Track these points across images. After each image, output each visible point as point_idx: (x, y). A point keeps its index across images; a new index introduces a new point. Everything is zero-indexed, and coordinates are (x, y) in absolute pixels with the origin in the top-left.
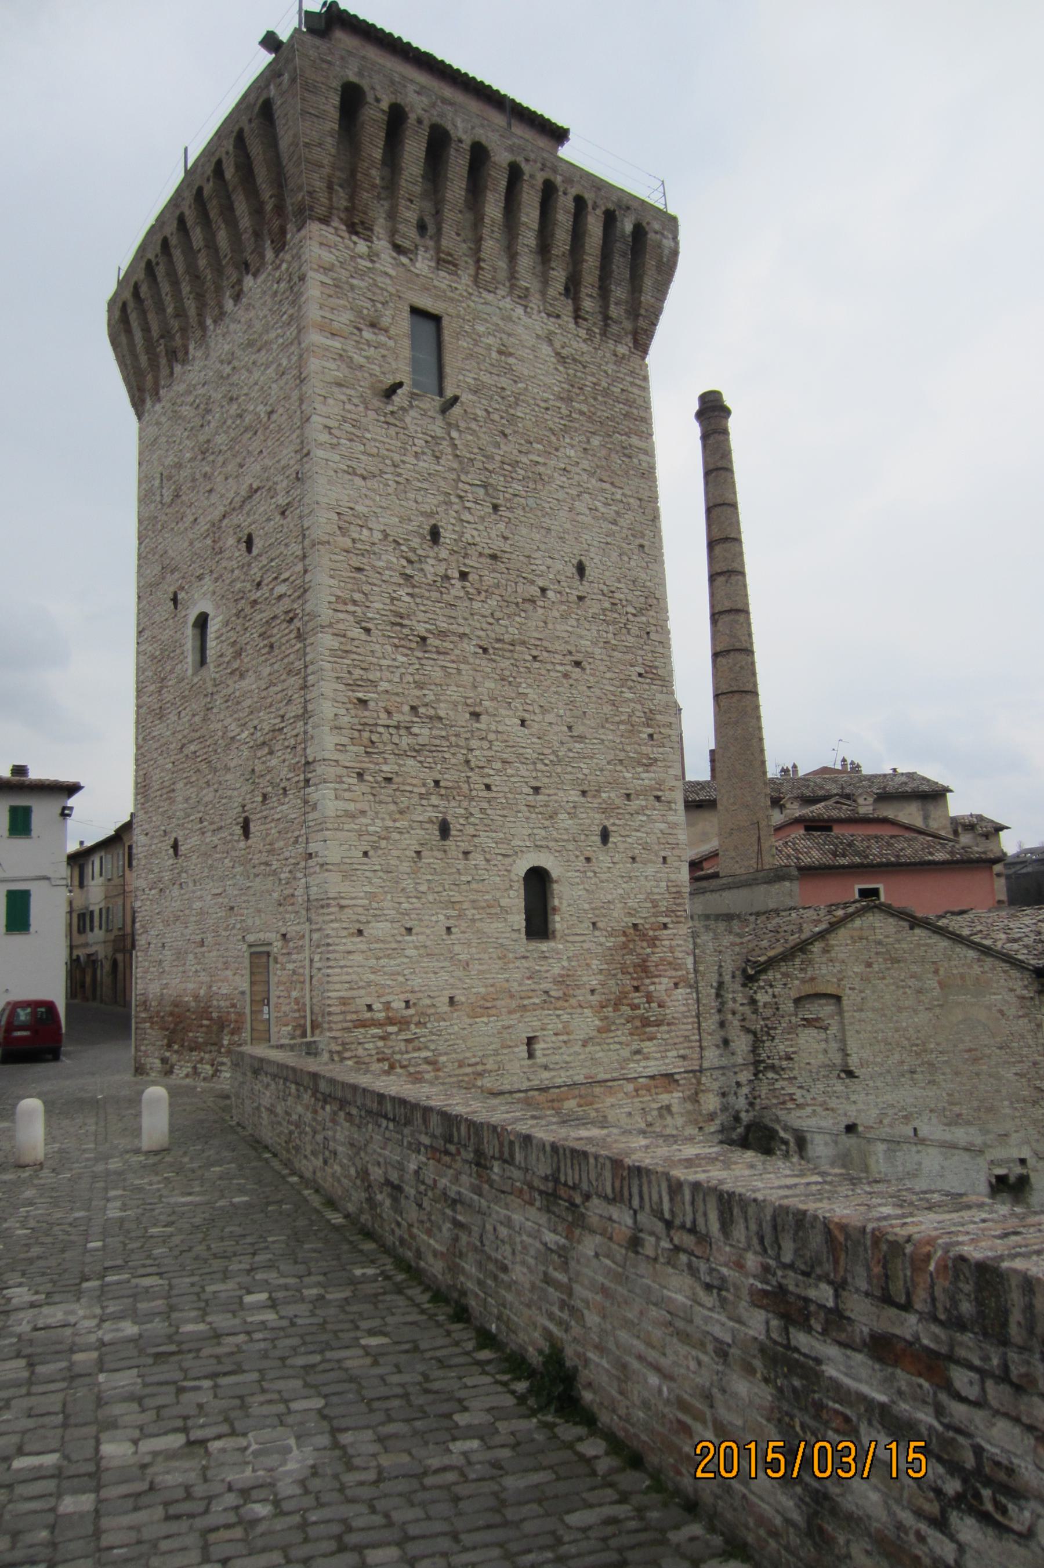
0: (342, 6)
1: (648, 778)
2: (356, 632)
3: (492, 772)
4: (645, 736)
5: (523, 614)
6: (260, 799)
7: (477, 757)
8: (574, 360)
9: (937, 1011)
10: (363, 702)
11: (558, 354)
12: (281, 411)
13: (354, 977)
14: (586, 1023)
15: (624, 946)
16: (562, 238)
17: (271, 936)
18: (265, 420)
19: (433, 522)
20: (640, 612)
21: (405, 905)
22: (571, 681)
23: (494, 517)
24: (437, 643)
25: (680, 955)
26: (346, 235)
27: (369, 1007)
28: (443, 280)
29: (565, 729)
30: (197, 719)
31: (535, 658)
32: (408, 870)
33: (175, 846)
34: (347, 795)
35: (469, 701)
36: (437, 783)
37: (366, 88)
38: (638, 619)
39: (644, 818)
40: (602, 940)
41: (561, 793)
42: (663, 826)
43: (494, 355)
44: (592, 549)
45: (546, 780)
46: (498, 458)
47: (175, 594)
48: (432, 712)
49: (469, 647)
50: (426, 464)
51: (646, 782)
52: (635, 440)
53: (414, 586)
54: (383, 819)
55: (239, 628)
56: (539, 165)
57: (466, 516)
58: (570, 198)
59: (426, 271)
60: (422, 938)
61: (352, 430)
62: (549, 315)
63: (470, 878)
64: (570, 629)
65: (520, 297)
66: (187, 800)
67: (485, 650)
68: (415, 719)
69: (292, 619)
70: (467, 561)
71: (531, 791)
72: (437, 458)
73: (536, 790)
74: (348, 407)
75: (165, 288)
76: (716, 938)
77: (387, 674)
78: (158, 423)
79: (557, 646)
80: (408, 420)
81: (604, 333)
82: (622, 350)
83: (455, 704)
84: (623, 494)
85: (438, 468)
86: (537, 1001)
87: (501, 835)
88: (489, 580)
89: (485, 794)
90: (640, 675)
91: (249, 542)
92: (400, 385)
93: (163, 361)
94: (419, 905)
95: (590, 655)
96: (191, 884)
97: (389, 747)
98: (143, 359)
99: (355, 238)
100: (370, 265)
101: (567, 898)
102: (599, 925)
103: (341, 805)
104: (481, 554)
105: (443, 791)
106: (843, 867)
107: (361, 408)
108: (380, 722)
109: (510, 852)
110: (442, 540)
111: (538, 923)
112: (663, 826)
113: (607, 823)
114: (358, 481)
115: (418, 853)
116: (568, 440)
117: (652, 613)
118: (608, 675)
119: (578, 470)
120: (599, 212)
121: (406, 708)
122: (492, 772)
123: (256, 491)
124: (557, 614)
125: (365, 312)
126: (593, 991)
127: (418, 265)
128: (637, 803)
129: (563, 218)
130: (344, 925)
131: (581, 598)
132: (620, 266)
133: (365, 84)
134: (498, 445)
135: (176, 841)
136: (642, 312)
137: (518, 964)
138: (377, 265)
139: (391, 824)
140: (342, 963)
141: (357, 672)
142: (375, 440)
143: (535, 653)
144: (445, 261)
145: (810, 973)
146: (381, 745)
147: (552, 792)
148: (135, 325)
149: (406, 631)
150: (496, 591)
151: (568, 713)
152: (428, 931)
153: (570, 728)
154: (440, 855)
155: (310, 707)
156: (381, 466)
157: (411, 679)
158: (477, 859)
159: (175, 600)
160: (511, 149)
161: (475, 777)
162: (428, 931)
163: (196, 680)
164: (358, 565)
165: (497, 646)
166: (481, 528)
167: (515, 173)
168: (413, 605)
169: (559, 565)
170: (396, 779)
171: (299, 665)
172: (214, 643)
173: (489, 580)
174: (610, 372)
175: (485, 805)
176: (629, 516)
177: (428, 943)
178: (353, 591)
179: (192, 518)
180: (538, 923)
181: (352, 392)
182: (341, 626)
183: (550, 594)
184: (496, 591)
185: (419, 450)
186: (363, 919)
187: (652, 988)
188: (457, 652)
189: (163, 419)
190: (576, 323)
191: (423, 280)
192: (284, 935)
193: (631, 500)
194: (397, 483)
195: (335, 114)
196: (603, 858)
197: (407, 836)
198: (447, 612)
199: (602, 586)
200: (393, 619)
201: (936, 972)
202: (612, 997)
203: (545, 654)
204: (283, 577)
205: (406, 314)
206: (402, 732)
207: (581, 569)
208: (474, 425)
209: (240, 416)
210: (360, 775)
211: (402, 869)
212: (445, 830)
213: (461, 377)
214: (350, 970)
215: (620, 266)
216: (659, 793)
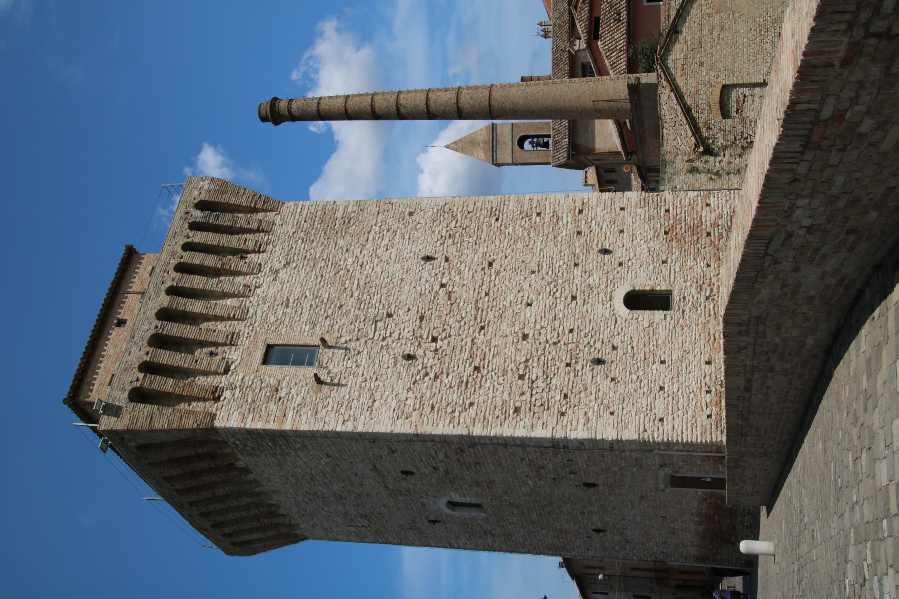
0: (65, 395)
2: (472, 411)
3: (561, 328)
4: (538, 218)
5: (458, 301)
6: (572, 476)
7: (552, 337)
8: (287, 255)
9: (737, 15)
10: (517, 410)
11: (284, 266)
12: (328, 449)
13: (689, 425)
15: (679, 241)
16: (210, 261)
17: (661, 473)
18: (331, 459)
19: (400, 358)
20: (454, 217)
21: (645, 389)
22: (502, 270)
23: (395, 317)
24: (478, 360)
25: (687, 201)
26: (220, 403)
27: (709, 416)
28: (244, 342)
29: (533, 275)
30: (516, 512)
31: (487, 294)
32: (623, 387)
33: (598, 531)
34: (574, 423)
35: (515, 341)
36: (568, 365)
37: (131, 387)
38: (459, 219)
39: (594, 222)
40: (674, 257)
41: (576, 281)
42: (599, 209)
43: (289, 310)
44: (413, 249)
45: (567, 291)
46: (357, 312)
47: (430, 521)
48: (522, 366)
49: (481, 338)
50: (363, 360)
51: (569, 219)
52: (339, 214)
53: (442, 373)
54: (590, 401)
55: (461, 482)
56: (165, 274)
57: (396, 335)
58: (184, 254)
59: (239, 352)
60: (666, 380)
61: (344, 406)
62: (260, 271)
63: (630, 347)
64: (467, 268)
65: (250, 291)
66: (568, 521)
67: (482, 328)
68: (527, 377)
69: (461, 450)
70: (425, 337)
71: (574, 302)
72: (359, 353)
73: (574, 298)
74: (330, 408)
75: (230, 516)
76: (676, 174)
77: (498, 394)
78: (313, 526)
79: (478, 278)
80: (335, 370)
81: (267, 232)
82: (278, 221)
83: (517, 350)
84: (376, 225)
85: (365, 353)
86: (712, 305)
87: (602, 324)
88: (437, 323)
89: (575, 333)
90: (497, 220)
91: (407, 473)
92: (316, 375)
93: (274, 520)
94: (645, 381)
95: (485, 254)
96: (624, 522)
97: (544, 394)
98: (269, 533)
99: (222, 398)
100: (238, 389)
101: (645, 280)
102: (664, 259)
103: (580, 427)
104: (420, 327)
105: (573, 361)
106: (629, 15)
107: (330, 400)
108: (529, 400)
109: (614, 318)
110: (412, 353)
112: (599, 209)
113: (596, 249)
114: (377, 404)
115: (612, 380)
116: (342, 263)
117: (455, 209)
118: (497, 243)
119: (361, 257)
120: (191, 234)
121: (520, 382)
122: (561, 328)
123: (375, 466)
124: (458, 277)
125: (268, 394)
126: (709, 266)
127: (235, 358)
128: (584, 228)
129: (197, 259)
130: (656, 429)
131: (447, 260)
132: (225, 219)
133: (129, 388)
134: (348, 312)
135: (594, 530)
136: (253, 205)
137: (687, 317)
138: (238, 385)
139: (593, 397)
140: (680, 433)
141: (497, 412)
142: (350, 392)
143: (483, 294)
144: (231, 341)
145: (704, 106)
146: (543, 400)
147: (575, 288)
148: (246, 538)
149: (470, 380)
150: (444, 318)
151: (523, 273)
152: (663, 376)
153: (533, 272)
154: (614, 366)
155: (519, 443)
156: (366, 390)
157: (501, 378)
158: (617, 341)
159: (434, 522)
160: (157, 293)
161: (564, 340)
162: (663, 376)
163: (490, 512)
164: (429, 408)
165: (479, 320)
166: (403, 326)
167: (173, 291)
168: (454, 374)
169: (425, 274)
170: (565, 391)
171: (491, 448)
172: (468, 498)
173: (437, 323)
174: (294, 230)
175: (582, 334)
176: (390, 221)
177: (670, 376)
178: (446, 412)
179: (383, 508)
181: (320, 405)
182: (468, 421)
183: (444, 281)
184: (444, 318)
185: (355, 364)
186: (652, 418)
187: (708, 223)
188: (483, 347)
189: (311, 523)
190: (263, 252)
191: (244, 356)
192: (661, 466)
193: (379, 220)
194: (376, 379)
195: (149, 407)
196: (619, 254)
197: (601, 387)
198: (458, 352)
199: (438, 244)
200: (463, 388)
201: (709, 15)
202: (712, 252)
203: (484, 287)
204: (433, 453)
205: (268, 368)
206: (535, 385)
207: (428, 259)
208: (336, 327)
209: (324, 474)
210: (563, 414)
211: (622, 391)
212: (599, 362)
213: (306, 334)
214: (685, 427)
215: (225, 219)
216: (577, 210)
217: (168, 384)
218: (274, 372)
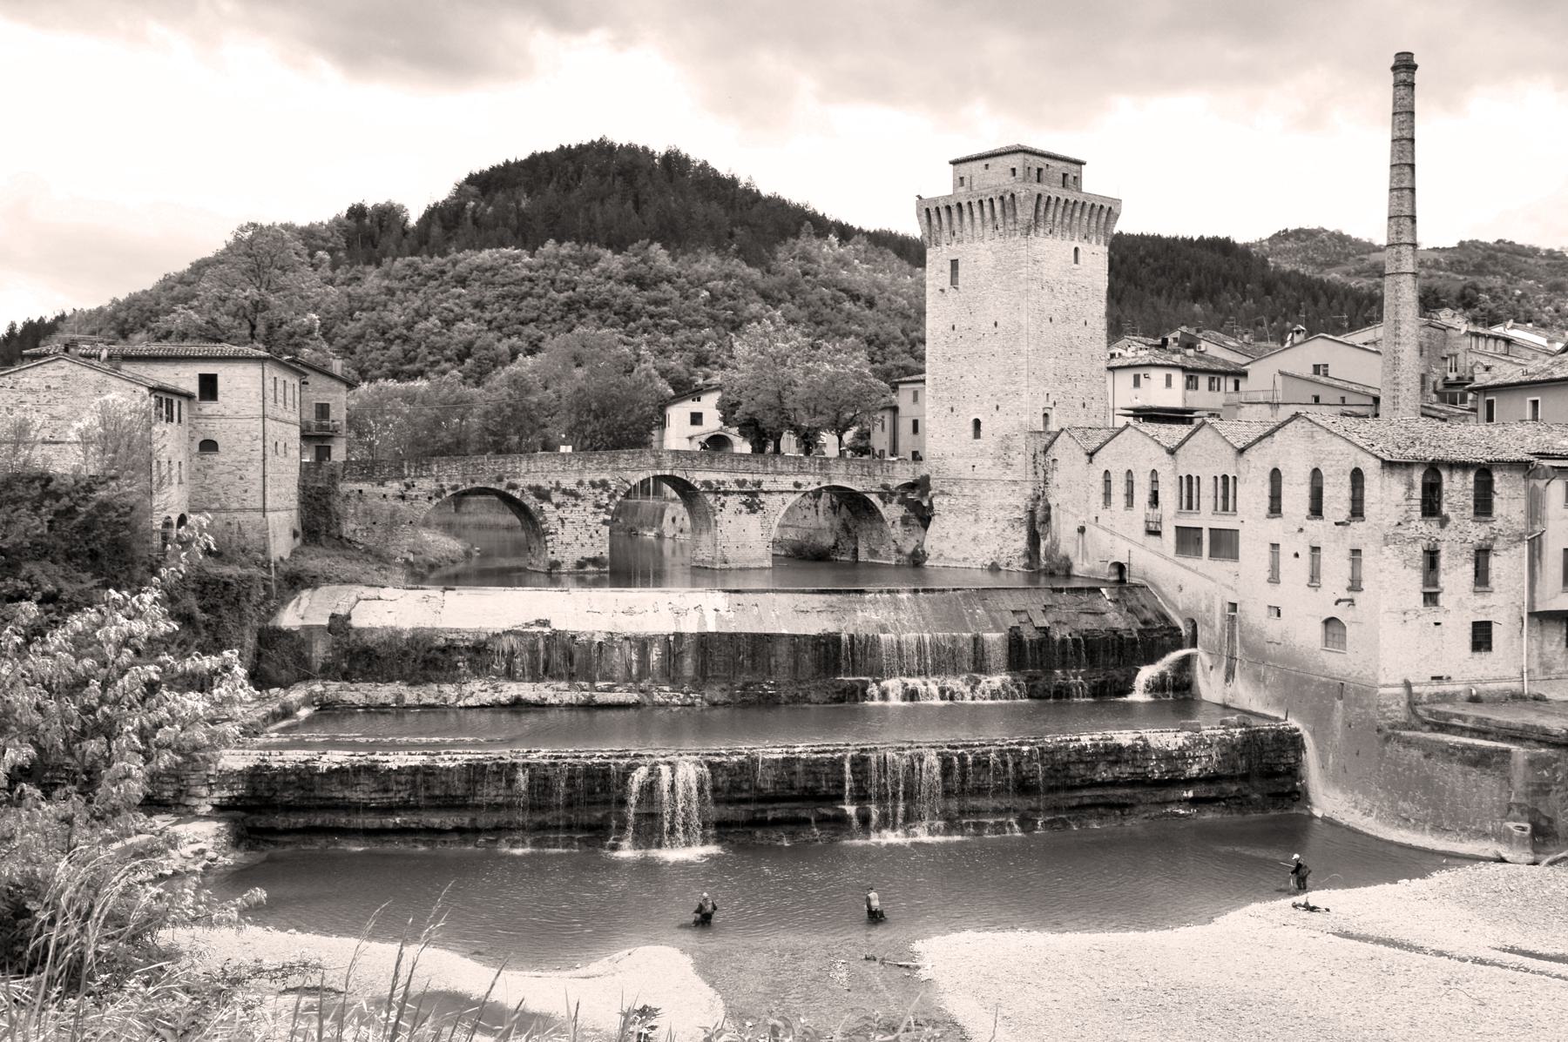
1: (1014, 388)
111: (977, 434)
132: (1009, 212)
180: (977, 434)
196: (997, 415)
217: (935, 221)
218: (948, 267)
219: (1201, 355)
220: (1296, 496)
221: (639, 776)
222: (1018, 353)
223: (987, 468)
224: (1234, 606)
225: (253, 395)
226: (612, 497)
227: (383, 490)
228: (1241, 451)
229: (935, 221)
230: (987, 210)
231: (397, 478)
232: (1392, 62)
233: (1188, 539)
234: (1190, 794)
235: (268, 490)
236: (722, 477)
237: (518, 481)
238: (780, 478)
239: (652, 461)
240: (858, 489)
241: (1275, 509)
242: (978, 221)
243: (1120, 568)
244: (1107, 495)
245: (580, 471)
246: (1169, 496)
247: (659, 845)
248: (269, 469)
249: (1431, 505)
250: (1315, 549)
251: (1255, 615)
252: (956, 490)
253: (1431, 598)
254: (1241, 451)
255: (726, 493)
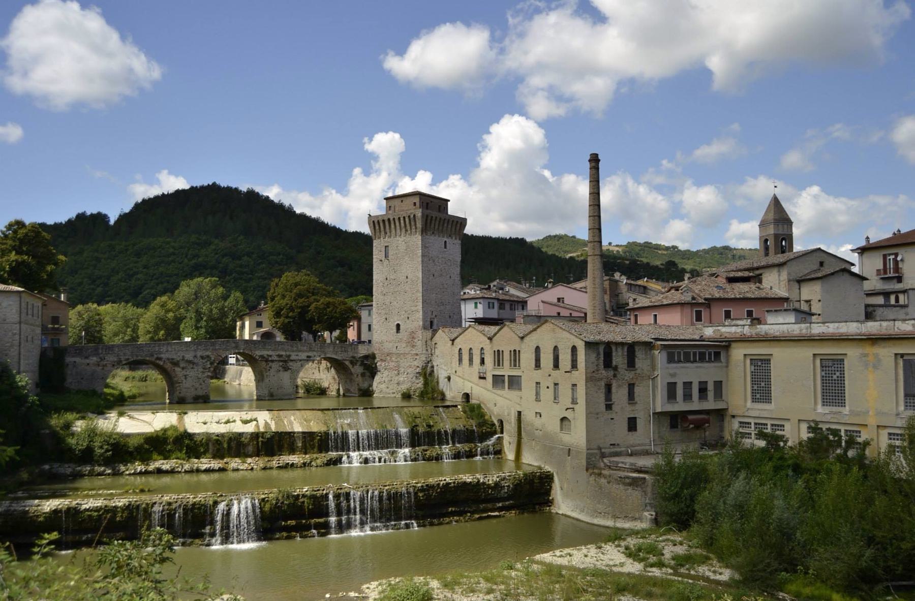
14: (404, 345)
101: (401, 327)
132: (413, 223)
218: (383, 249)
219: (507, 293)
220: (547, 359)
221: (222, 507)
222: (418, 291)
223: (403, 348)
224: (519, 413)
225: (14, 311)
226: (212, 364)
227: (88, 361)
228: (522, 338)
229: (377, 227)
230: (402, 222)
231: (95, 355)
232: (589, 158)
233: (498, 380)
234: (500, 505)
235: (22, 361)
236: (270, 353)
237: (162, 356)
238: (300, 354)
239: (234, 345)
240: (340, 358)
241: (538, 365)
242: (398, 227)
243: (467, 396)
244: (460, 360)
245: (195, 351)
246: (489, 360)
247: (232, 543)
248: (22, 350)
249: (608, 364)
250: (556, 384)
251: (529, 416)
252: (388, 358)
253: (609, 407)
254: (522, 338)
255: (272, 361)
